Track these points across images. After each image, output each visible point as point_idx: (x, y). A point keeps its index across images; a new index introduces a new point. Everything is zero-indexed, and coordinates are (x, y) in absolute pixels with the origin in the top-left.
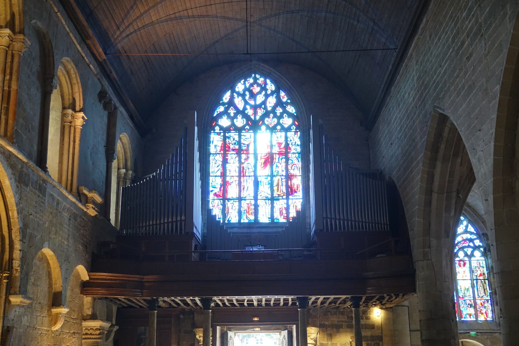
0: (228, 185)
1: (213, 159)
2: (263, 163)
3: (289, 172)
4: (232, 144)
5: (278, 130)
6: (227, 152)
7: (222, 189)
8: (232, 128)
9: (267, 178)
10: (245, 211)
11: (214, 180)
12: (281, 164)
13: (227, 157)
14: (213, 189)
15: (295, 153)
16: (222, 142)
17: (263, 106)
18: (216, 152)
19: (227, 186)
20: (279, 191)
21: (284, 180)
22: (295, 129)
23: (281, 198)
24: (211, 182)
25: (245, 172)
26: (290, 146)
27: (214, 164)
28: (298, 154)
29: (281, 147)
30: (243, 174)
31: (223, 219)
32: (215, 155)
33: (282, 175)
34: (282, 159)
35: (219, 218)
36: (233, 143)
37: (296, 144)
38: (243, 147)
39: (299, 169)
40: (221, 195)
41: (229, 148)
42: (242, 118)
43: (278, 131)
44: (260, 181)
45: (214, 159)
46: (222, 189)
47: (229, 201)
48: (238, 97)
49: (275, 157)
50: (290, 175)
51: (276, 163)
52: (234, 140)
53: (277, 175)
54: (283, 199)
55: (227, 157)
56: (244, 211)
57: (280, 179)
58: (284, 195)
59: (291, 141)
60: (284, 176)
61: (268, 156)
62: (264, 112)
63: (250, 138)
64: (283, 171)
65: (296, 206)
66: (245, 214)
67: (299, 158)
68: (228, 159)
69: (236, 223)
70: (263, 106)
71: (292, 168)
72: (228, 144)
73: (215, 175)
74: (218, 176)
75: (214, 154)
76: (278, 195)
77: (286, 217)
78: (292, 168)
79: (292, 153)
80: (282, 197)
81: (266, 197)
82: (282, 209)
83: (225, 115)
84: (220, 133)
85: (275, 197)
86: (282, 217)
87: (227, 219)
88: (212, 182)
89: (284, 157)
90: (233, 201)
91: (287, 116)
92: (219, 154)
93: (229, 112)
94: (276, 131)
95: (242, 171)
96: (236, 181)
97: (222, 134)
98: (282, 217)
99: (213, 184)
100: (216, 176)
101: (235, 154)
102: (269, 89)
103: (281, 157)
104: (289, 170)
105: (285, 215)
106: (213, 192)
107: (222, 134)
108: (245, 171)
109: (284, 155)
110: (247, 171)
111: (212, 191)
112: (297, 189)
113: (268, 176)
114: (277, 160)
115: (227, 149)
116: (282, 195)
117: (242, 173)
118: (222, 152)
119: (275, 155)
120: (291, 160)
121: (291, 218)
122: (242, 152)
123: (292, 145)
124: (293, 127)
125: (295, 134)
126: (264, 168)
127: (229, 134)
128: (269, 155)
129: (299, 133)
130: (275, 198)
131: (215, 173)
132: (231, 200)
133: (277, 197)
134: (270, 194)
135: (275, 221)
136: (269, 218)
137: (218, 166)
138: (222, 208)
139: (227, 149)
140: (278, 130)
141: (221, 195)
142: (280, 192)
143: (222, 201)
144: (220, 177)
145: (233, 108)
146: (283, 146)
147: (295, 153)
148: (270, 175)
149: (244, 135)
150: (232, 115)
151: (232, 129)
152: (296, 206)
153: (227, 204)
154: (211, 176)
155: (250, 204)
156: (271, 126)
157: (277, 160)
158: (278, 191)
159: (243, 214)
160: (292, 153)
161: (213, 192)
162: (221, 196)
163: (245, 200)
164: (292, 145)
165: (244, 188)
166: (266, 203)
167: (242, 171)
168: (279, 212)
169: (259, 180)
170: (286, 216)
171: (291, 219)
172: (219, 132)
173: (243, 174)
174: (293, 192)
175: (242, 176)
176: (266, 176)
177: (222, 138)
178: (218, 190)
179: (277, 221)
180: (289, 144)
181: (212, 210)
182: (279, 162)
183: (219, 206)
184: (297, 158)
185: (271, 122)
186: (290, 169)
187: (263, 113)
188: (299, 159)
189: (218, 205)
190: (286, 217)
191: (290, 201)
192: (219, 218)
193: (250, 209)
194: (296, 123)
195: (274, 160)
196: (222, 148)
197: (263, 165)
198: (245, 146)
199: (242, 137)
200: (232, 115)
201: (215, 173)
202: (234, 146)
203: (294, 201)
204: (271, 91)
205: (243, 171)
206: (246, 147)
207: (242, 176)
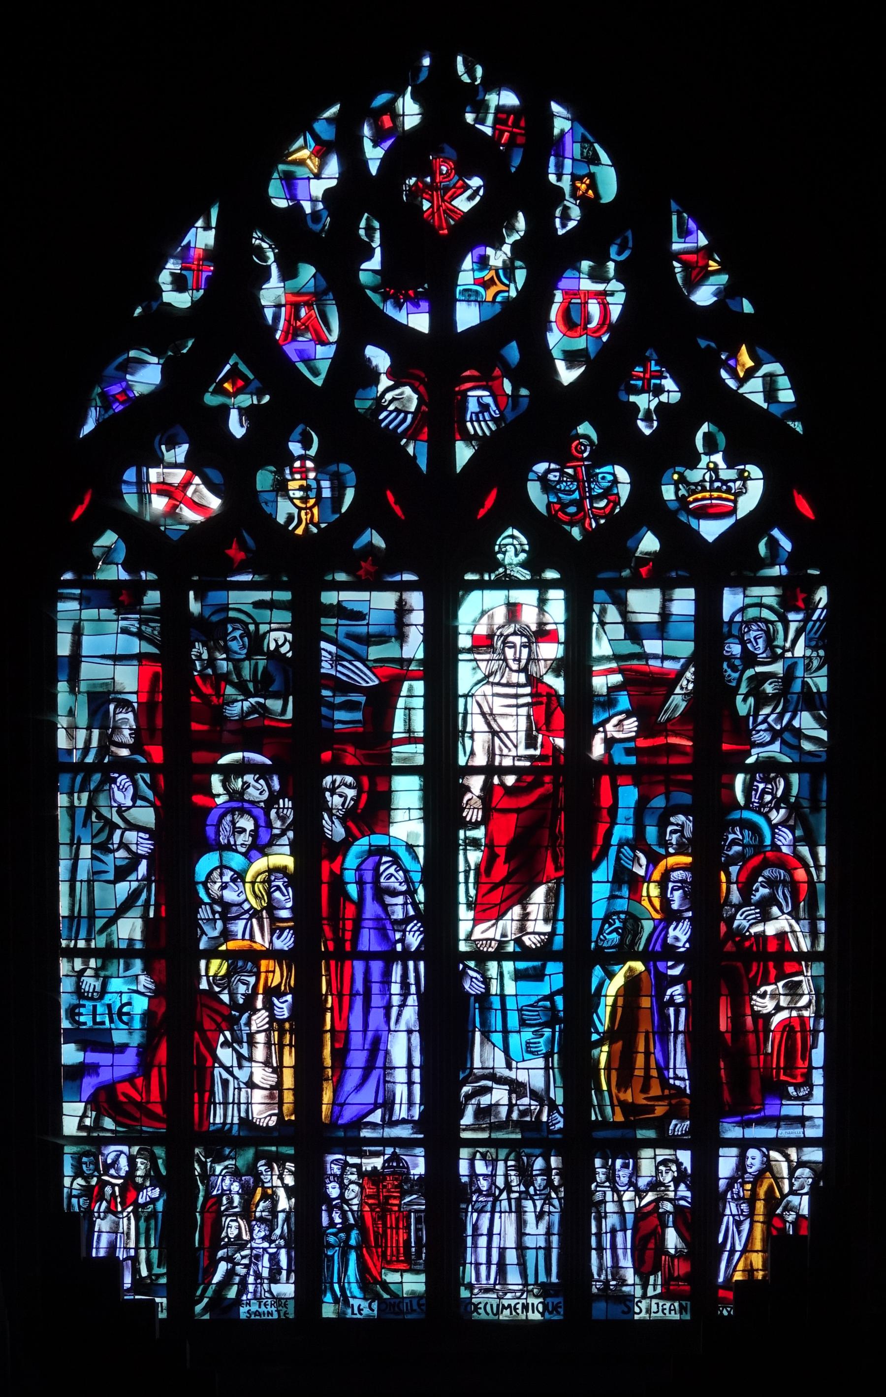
0: (208, 1024)
1: (80, 815)
2: (501, 852)
3: (723, 928)
4: (241, 686)
5: (644, 571)
6: (199, 757)
7: (162, 1054)
8: (243, 546)
9: (538, 975)
10: (354, 1234)
11: (90, 983)
12: (654, 859)
13: (199, 799)
14: (93, 1057)
15: (783, 770)
16: (158, 668)
17: (513, 352)
18: (103, 749)
19: (202, 1032)
20: (638, 1084)
21: (676, 992)
22: (791, 561)
23: (651, 1134)
24: (66, 1000)
25: (349, 925)
26: (743, 707)
27: (86, 851)
28: (807, 776)
29: (663, 718)
30: (339, 941)
31: (170, 1291)
32: (97, 777)
33: (669, 952)
34: (663, 823)
35: (139, 1284)
36: (246, 673)
37: (797, 687)
38: (339, 715)
39: (812, 907)
40: (158, 1109)
41: (217, 714)
42: (321, 462)
43: (636, 573)
44: (484, 998)
45: (91, 806)
46: (162, 1054)
47: (219, 1158)
48: (288, 273)
49: (606, 801)
50: (729, 947)
51: (613, 851)
52: (256, 642)
53: (623, 954)
54: (665, 1141)
55: (199, 799)
56: (347, 1228)
57: (647, 984)
58: (674, 1113)
59: (750, 659)
60: (679, 958)
61: (548, 787)
62: (525, 403)
63: (392, 630)
64: (670, 916)
65: (772, 1201)
66: (353, 1257)
67: (815, 808)
68: (207, 811)
69: (281, 1323)
70: (513, 352)
71: (746, 891)
72: (207, 690)
73: (100, 942)
74: (129, 953)
75: (87, 770)
76: (627, 1108)
77: (684, 1286)
78: (746, 891)
79: (750, 770)
80: (661, 1124)
81: (519, 1125)
82: (654, 1221)
83: (182, 433)
84: (138, 588)
85: (605, 1124)
86: (656, 1281)
87: (209, 1293)
88: (74, 1000)
89: (685, 798)
90: (250, 1153)
91: (721, 439)
92: (128, 768)
93: (211, 400)
94: (626, 573)
95: (325, 911)
96: (272, 993)
97: (153, 597)
98: (656, 1281)
99: (85, 1019)
100: (109, 954)
101: (262, 772)
102: (567, 189)
103: (659, 802)
104: (727, 911)
105: (682, 1268)
106: (89, 1085)
107: (153, 597)
108: (350, 911)
109: (684, 786)
110: (371, 909)
111: (79, 1071)
112: (790, 1067)
113: (544, 953)
114: (623, 831)
115: (195, 726)
116: (660, 1111)
117: (327, 929)
118: (157, 753)
119: (606, 780)
120: (747, 824)
121: (730, 1295)
122: (327, 756)
123: (762, 700)
124: (773, 544)
125: (787, 604)
126: (508, 889)
127: (216, 597)
128: (555, 782)
129: (822, 595)
130: (600, 1134)
131: (99, 923)
132: (239, 1144)
133: (616, 1125)
134: (558, 1095)
135: (599, 1310)
136: (546, 1290)
137: (122, 873)
138: (160, 1206)
139: (195, 726)
140: (644, 571)
141: (158, 1109)
142: (645, 1088)
143: (160, 1151)
144: (138, 965)
145: (243, 367)
146: (678, 702)
147: (783, 770)
148: (558, 943)
149: (340, 611)
150: (237, 428)
151: (235, 553)
152: (772, 1201)
153: (206, 1176)
154: (72, 954)
155: (389, 1182)
156: (576, 532)
157: (623, 831)
158: (625, 1081)
159: (335, 1253)
160: (750, 770)
161: (89, 1085)
162: (152, 1116)
163: (357, 1147)
164: (762, 700)
165: (341, 1055)
166: (526, 1176)
167: (325, 911)
168: (625, 1240)
169: (472, 985)
170: (687, 1278)
171: (725, 1303)
172: (124, 576)
173: (339, 941)
174: (755, 1089)
175: (327, 956)
176: (524, 953)
177: (153, 629)
178: (127, 1062)
179: (616, 1312)
180: (735, 690)
181: (85, 1226)
182: (638, 842)
183: (141, 1188)
184: (794, 809)
185: (576, 495)
186: (736, 897)
187: (510, 416)
188: (812, 819)
189: (130, 1184)
190: (684, 1286)
191: (726, 1165)
192: (139, 1284)
193: (391, 1220)
194: (804, 507)
195: (602, 828)
196: (159, 722)
197: (501, 870)
198: (350, 706)
199: (328, 623)
200: (237, 428)
201: (99, 923)
202: (253, 700)
203: (754, 1157)
204: (590, 205)
205: (335, 918)
206: (358, 716)
207: (327, 956)
